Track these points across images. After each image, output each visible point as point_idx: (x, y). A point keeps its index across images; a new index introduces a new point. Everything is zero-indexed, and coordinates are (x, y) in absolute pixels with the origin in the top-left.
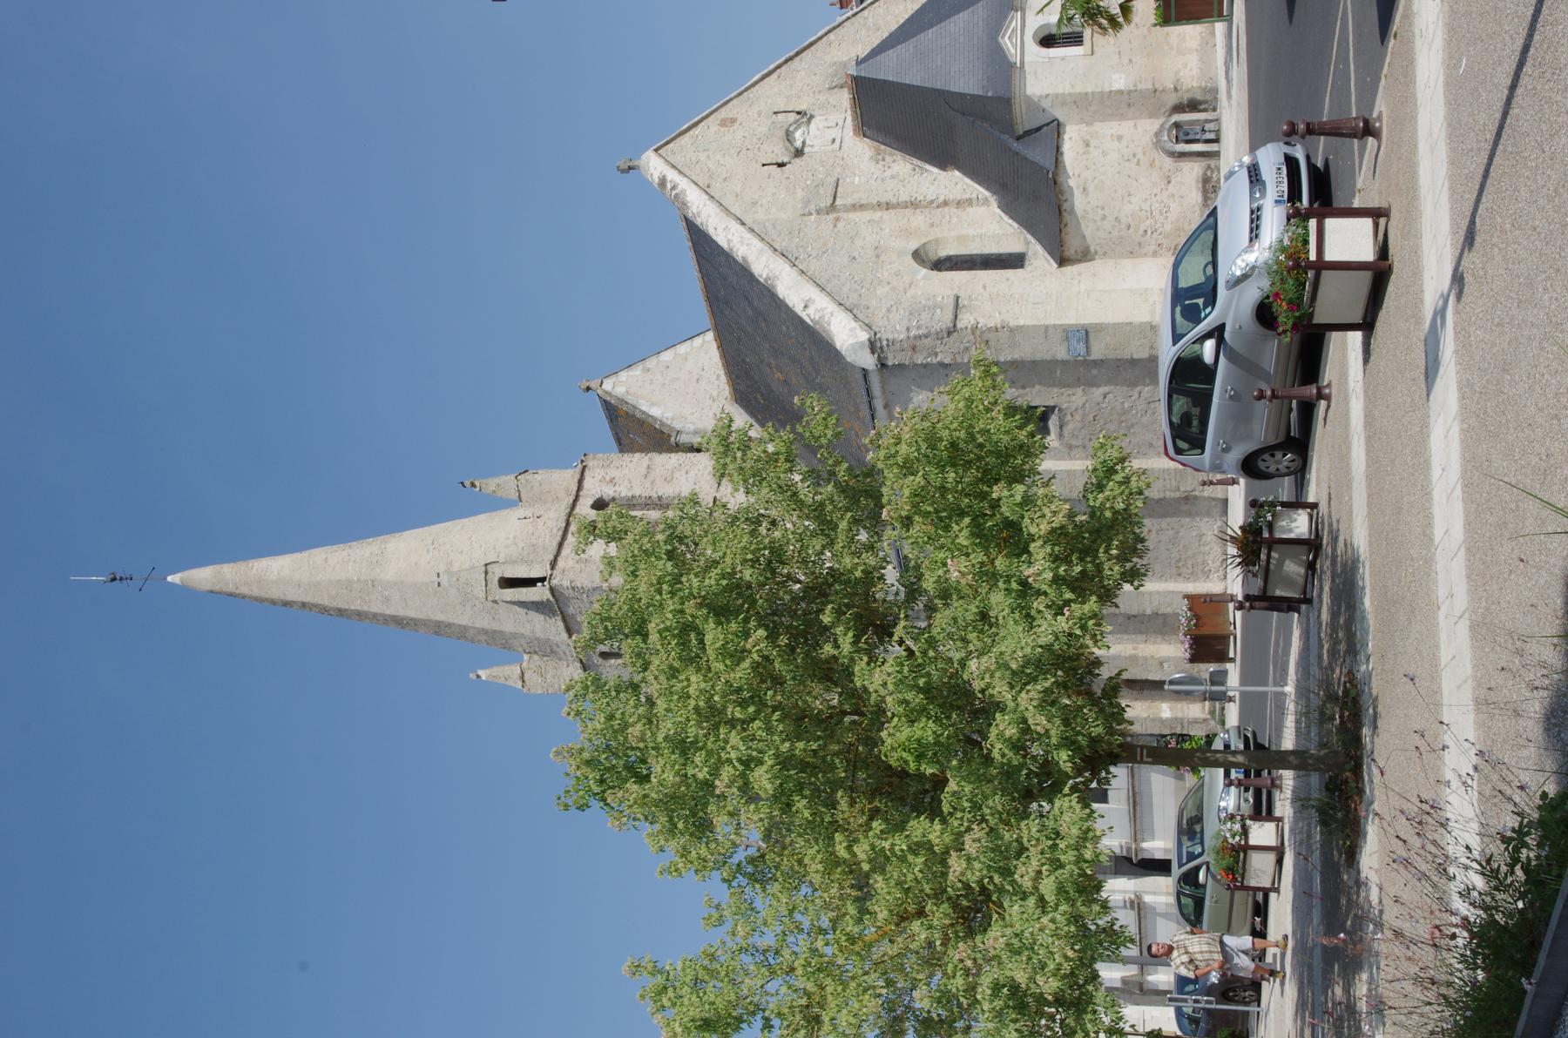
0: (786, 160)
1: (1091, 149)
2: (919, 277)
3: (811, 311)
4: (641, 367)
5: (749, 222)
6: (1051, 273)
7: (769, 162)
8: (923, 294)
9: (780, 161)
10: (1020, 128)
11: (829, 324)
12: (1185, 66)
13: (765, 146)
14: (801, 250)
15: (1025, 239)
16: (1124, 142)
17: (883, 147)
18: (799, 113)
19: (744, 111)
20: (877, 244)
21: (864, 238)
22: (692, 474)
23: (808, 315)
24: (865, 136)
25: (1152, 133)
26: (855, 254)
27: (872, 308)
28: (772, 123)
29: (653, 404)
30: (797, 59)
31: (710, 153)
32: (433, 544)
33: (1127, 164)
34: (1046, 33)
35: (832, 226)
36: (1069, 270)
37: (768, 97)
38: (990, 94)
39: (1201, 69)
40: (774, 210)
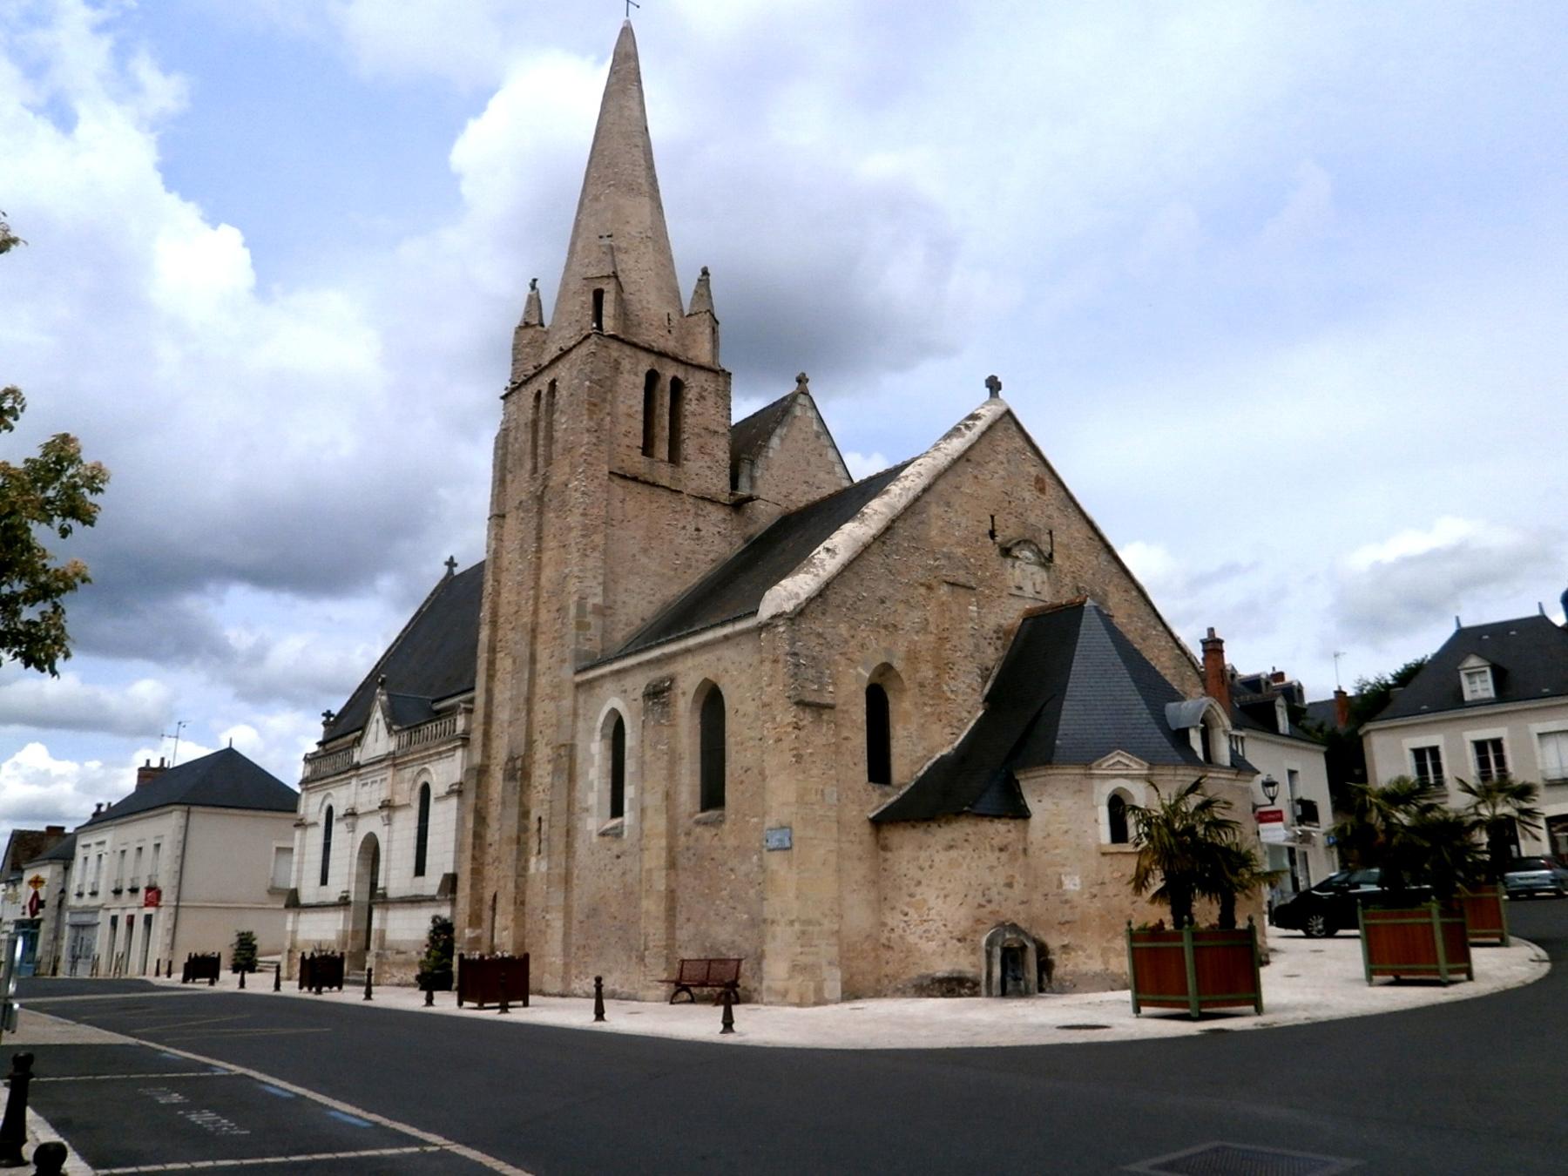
0: (998, 539)
1: (997, 854)
2: (860, 670)
3: (823, 555)
4: (821, 430)
5: (928, 498)
6: (862, 811)
7: (996, 522)
8: (839, 672)
9: (997, 533)
10: (1023, 776)
11: (806, 573)
12: (1090, 957)
13: (1014, 520)
14: (894, 547)
15: (905, 784)
16: (1006, 891)
17: (1012, 638)
18: (1051, 555)
19: (1053, 502)
20: (900, 627)
21: (907, 614)
22: (709, 473)
23: (819, 553)
24: (1024, 620)
25: (1015, 921)
26: (888, 604)
27: (823, 618)
28: (1040, 529)
29: (782, 440)
30: (1109, 558)
31: (1006, 465)
32: (647, 237)
33: (980, 893)
34: (1123, 797)
35: (922, 581)
36: (867, 829)
37: (1069, 526)
38: (1058, 742)
39: (1086, 974)
40: (941, 523)
